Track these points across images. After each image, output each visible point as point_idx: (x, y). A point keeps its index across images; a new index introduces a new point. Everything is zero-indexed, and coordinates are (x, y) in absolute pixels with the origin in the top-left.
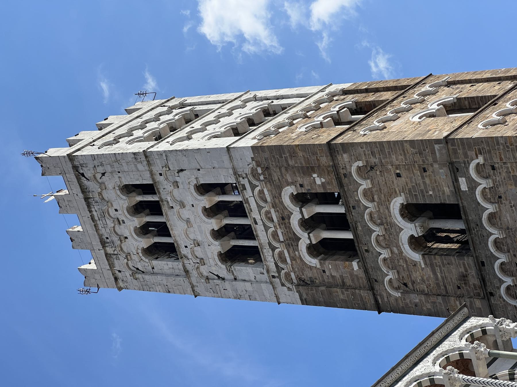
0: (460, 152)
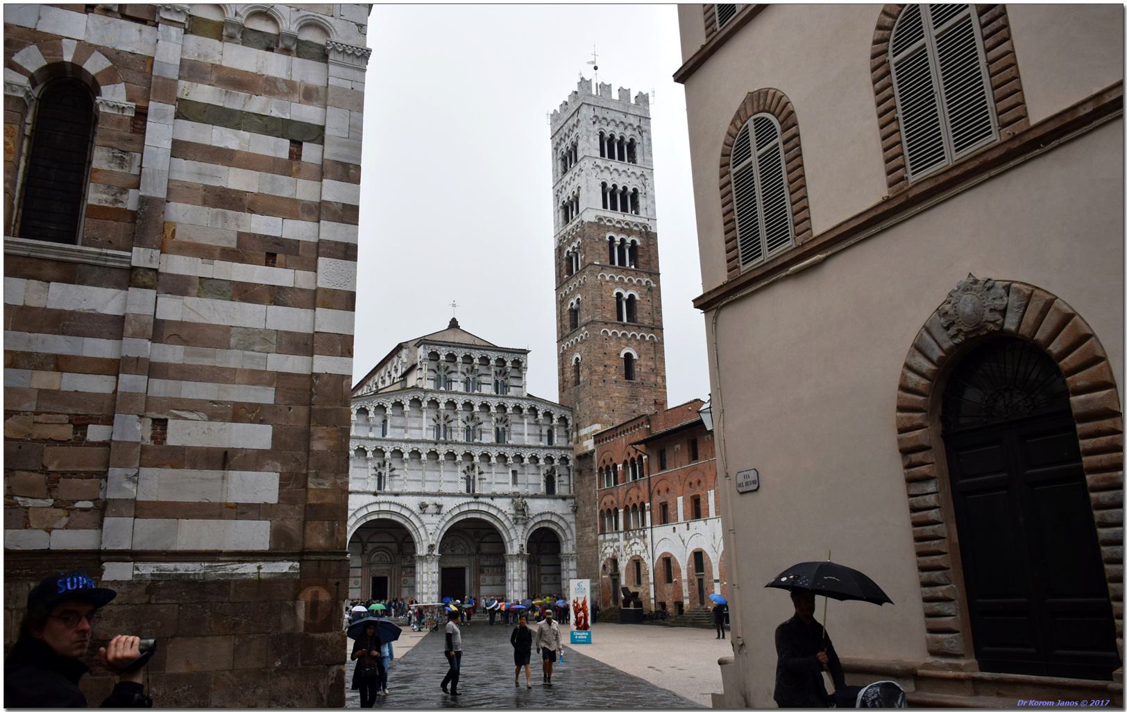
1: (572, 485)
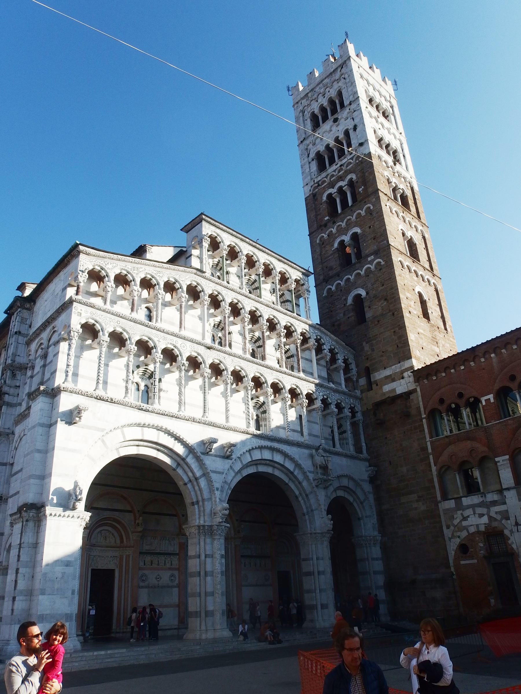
0: (385, 253)
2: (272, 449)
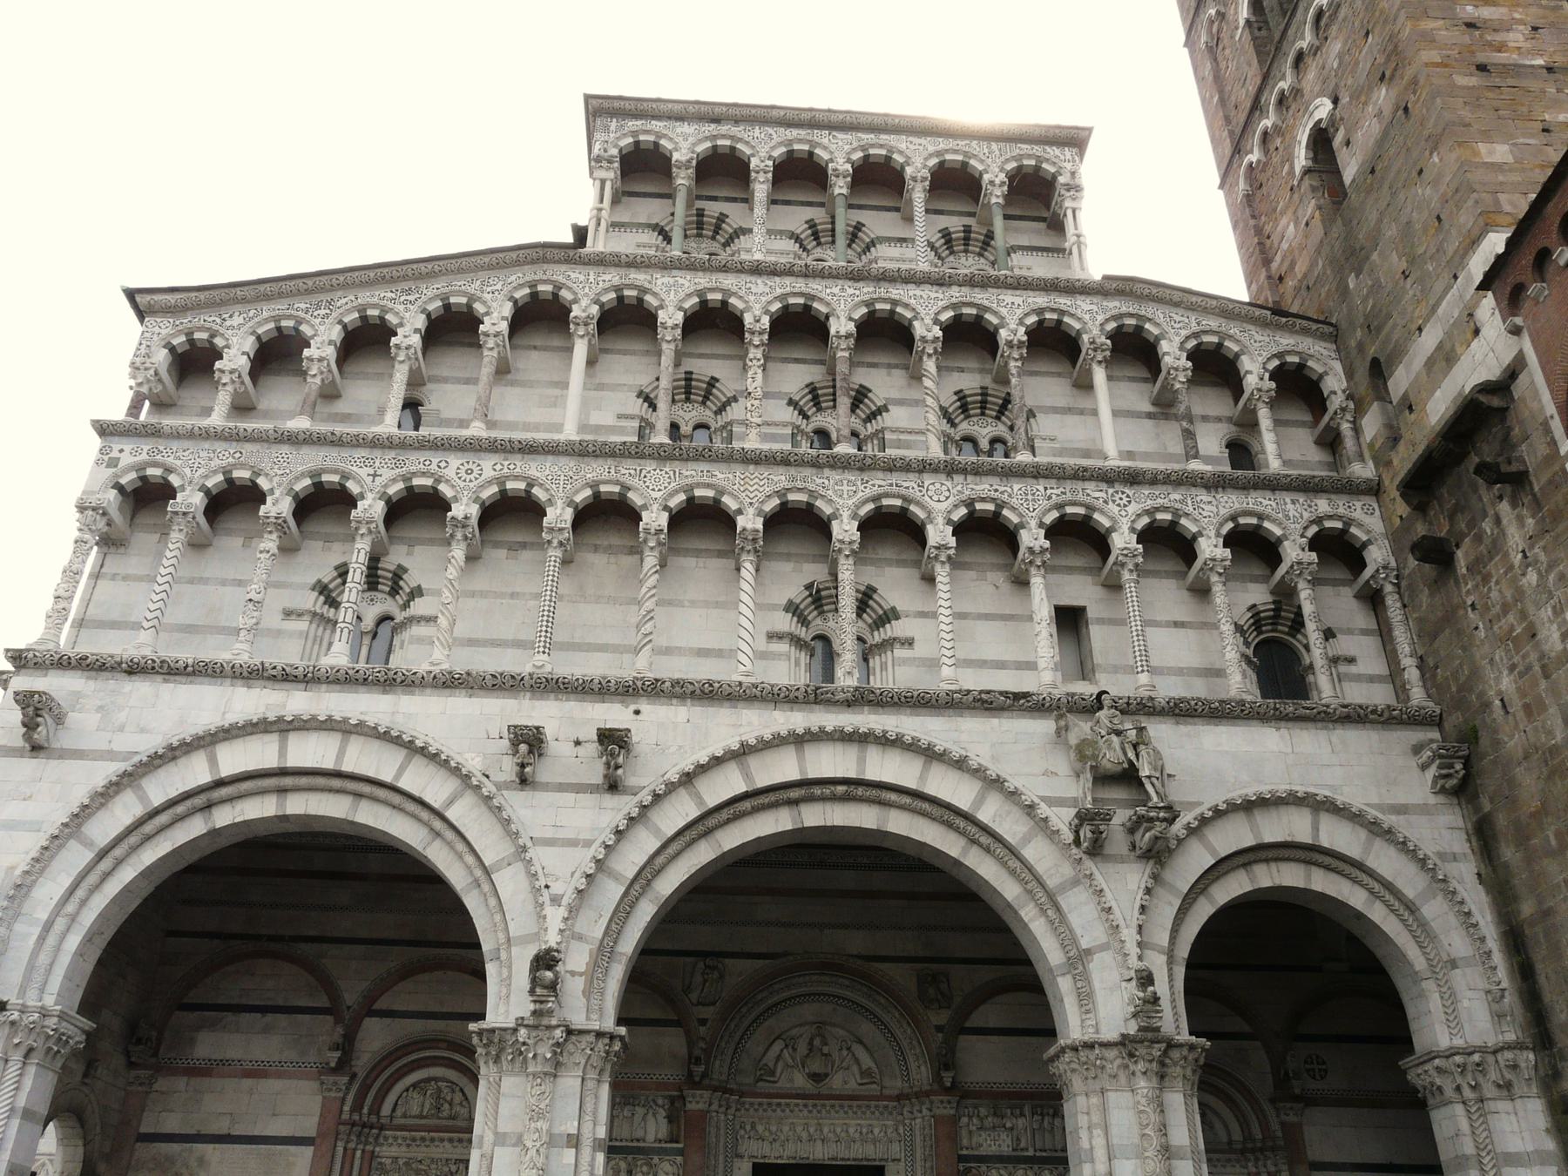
1: (1408, 662)
2: (860, 739)
